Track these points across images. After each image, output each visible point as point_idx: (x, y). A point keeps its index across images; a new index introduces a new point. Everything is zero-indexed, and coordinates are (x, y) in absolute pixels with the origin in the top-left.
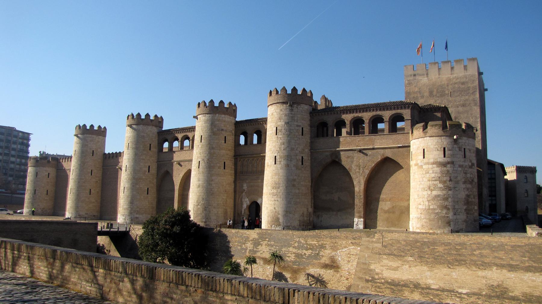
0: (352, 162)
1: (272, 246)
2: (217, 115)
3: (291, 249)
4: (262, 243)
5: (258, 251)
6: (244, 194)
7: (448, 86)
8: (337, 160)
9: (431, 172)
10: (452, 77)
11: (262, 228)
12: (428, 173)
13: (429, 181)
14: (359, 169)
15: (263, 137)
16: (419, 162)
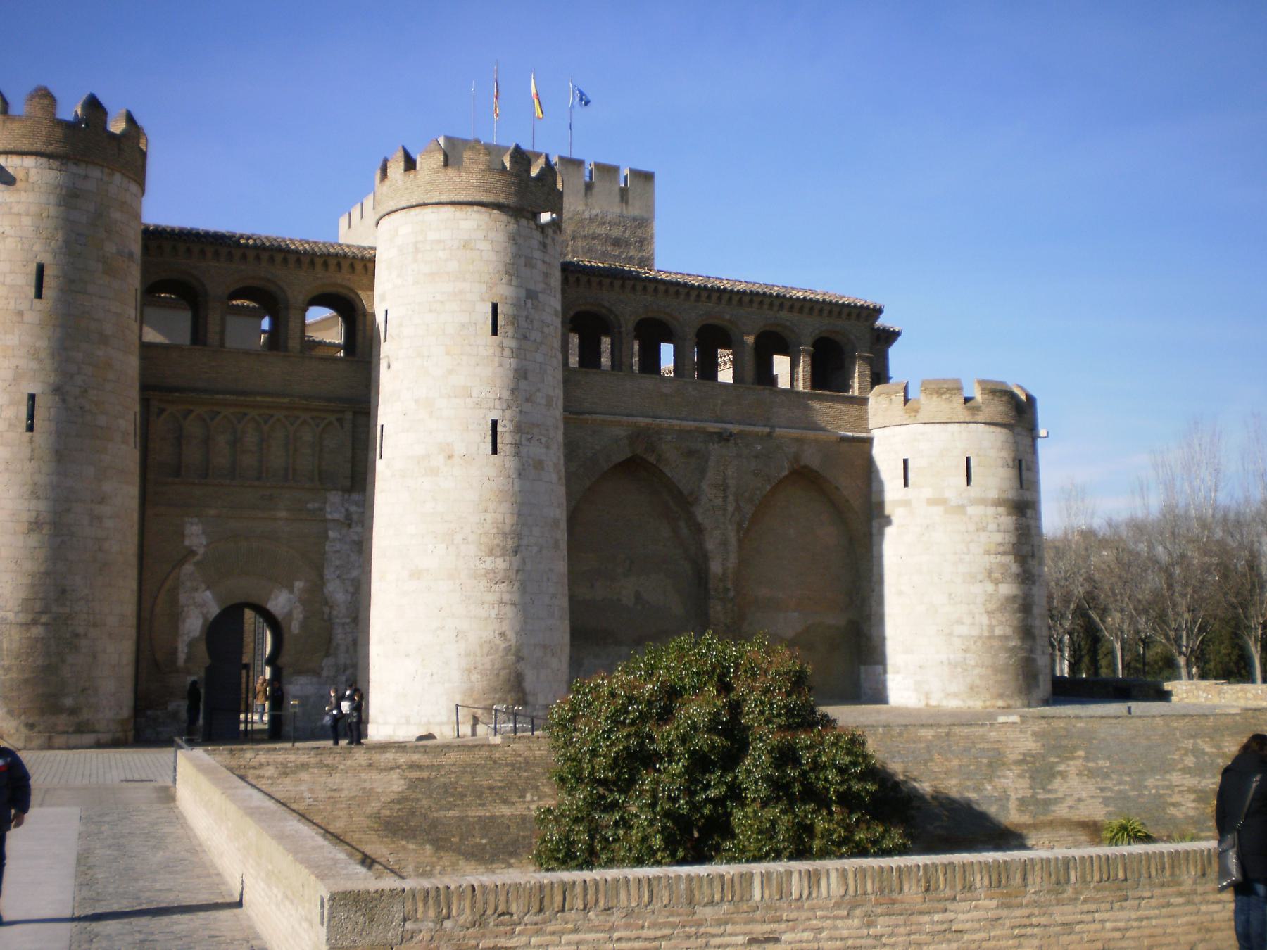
0: (703, 472)
1: (1106, 776)
2: (118, 177)
3: (1175, 778)
4: (1062, 767)
5: (1057, 801)
6: (188, 568)
7: (574, 238)
8: (652, 459)
9: (993, 526)
10: (586, 215)
11: (385, 723)
12: (984, 529)
13: (988, 553)
14: (725, 499)
15: (360, 326)
16: (950, 494)
